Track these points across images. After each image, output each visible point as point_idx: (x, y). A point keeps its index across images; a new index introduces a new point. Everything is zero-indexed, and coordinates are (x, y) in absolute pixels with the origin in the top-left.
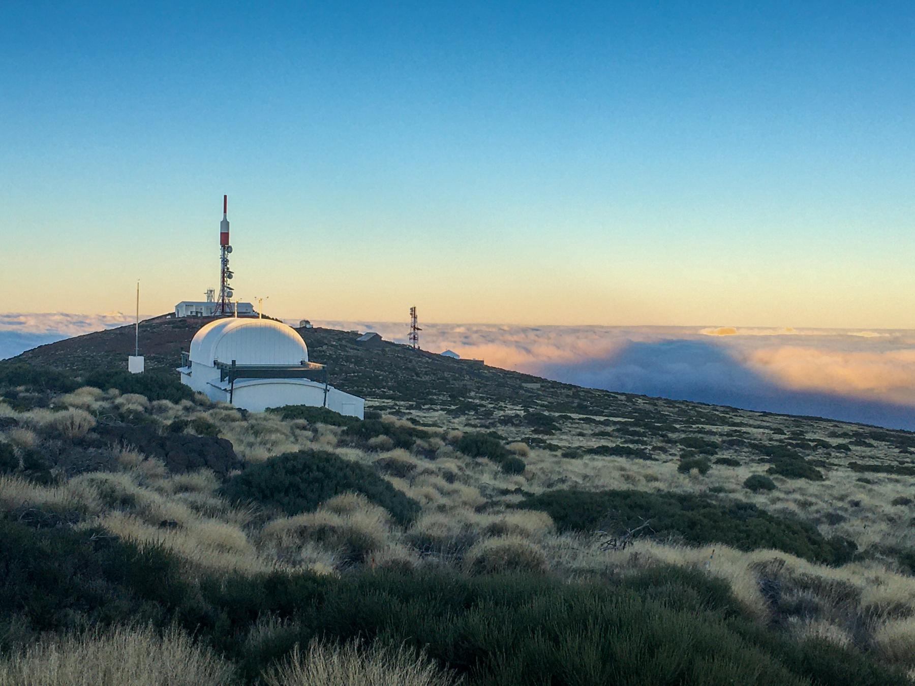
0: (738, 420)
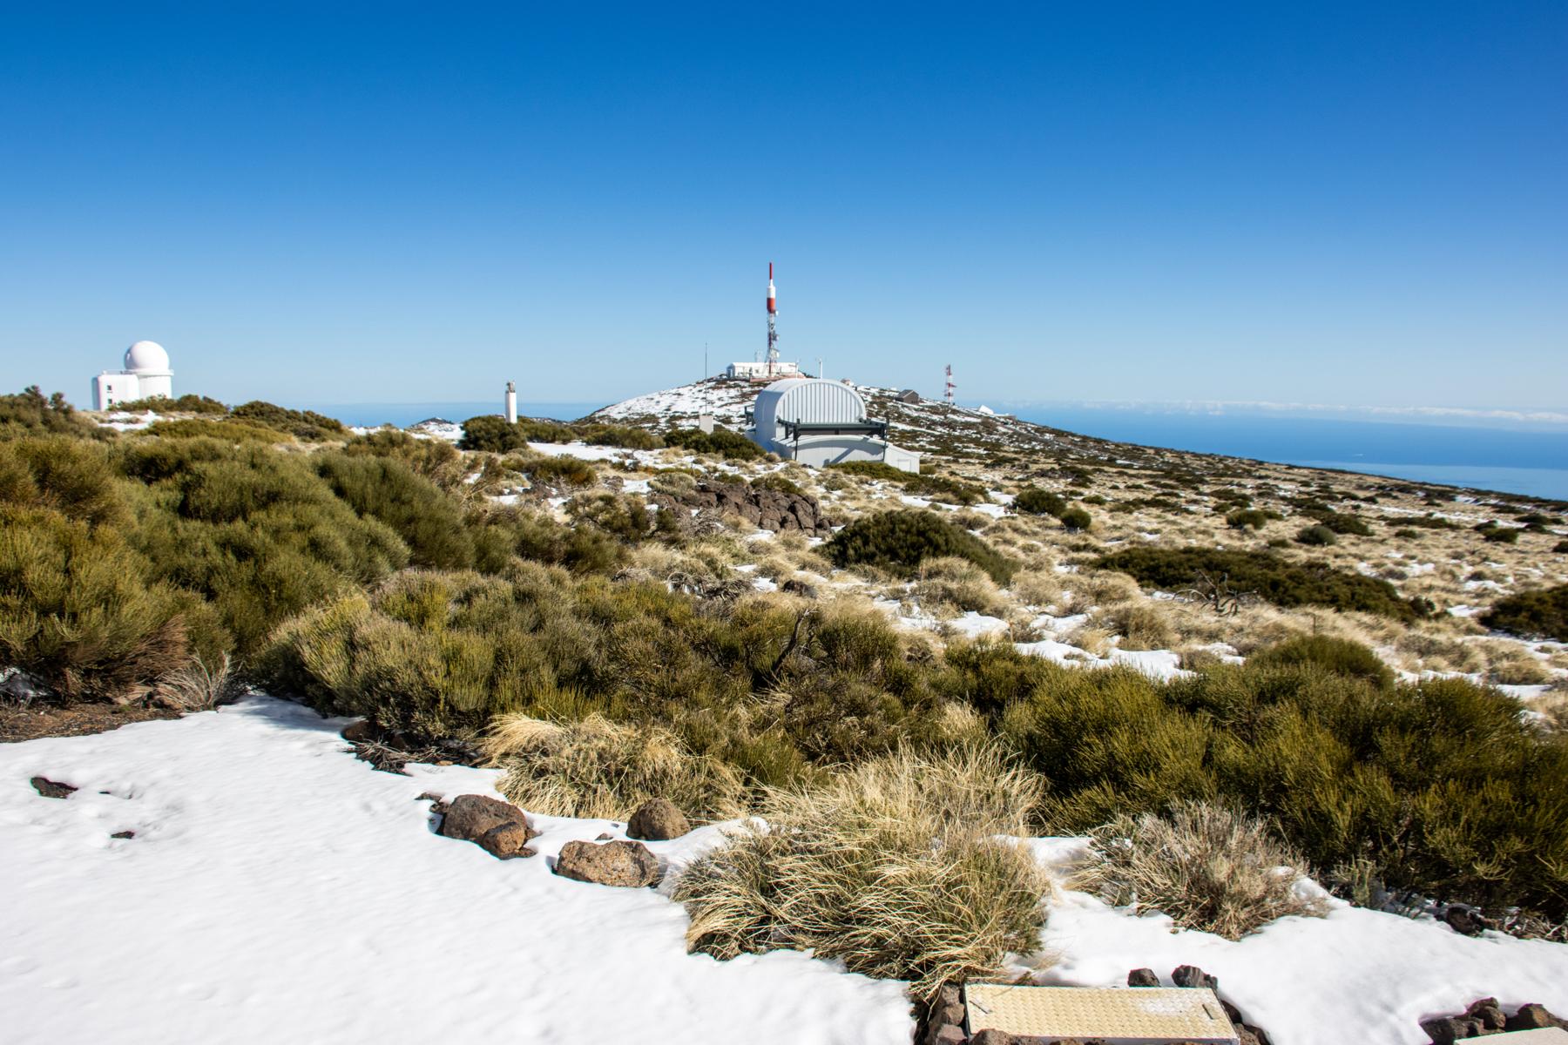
0: (1263, 473)
